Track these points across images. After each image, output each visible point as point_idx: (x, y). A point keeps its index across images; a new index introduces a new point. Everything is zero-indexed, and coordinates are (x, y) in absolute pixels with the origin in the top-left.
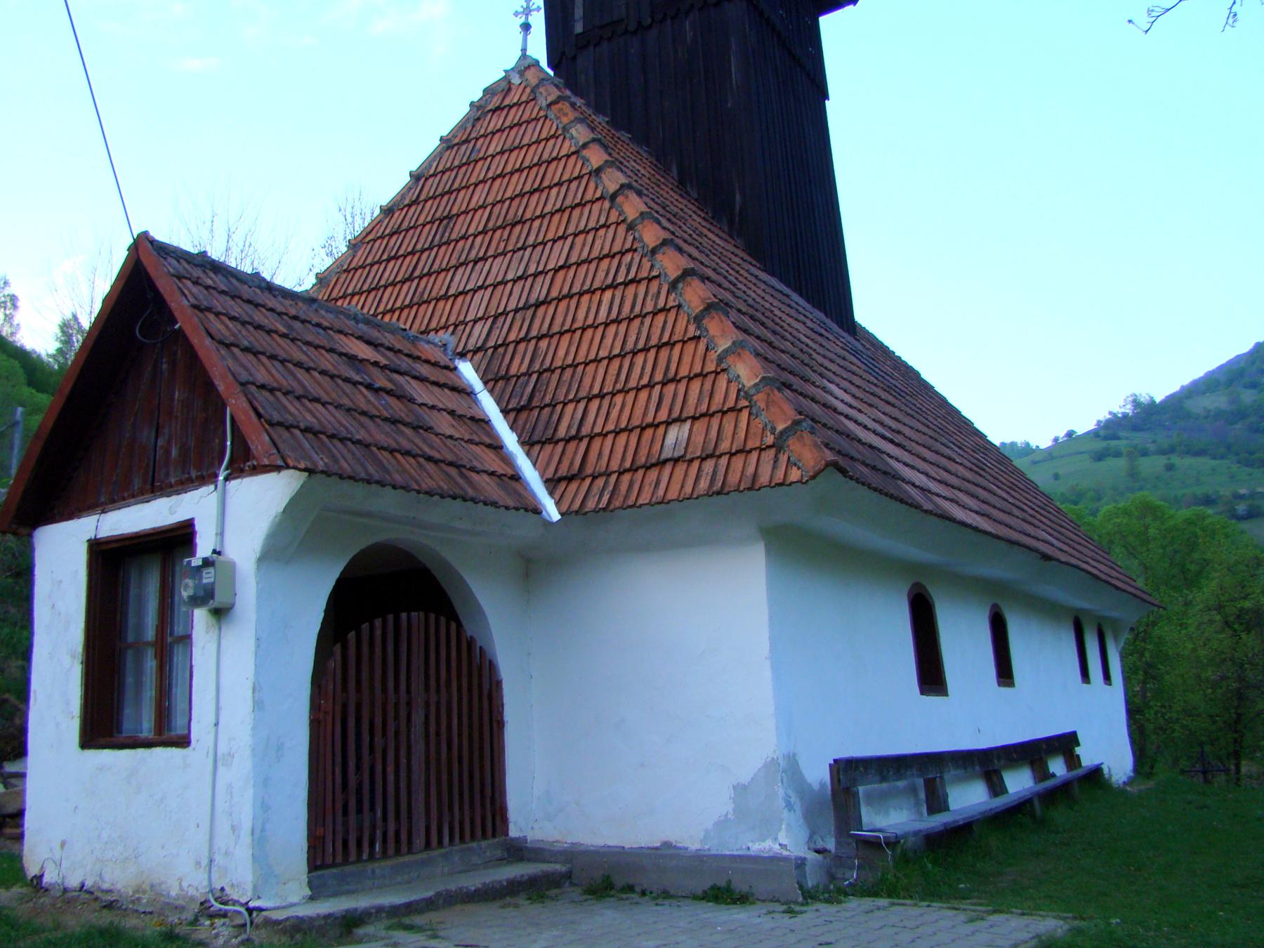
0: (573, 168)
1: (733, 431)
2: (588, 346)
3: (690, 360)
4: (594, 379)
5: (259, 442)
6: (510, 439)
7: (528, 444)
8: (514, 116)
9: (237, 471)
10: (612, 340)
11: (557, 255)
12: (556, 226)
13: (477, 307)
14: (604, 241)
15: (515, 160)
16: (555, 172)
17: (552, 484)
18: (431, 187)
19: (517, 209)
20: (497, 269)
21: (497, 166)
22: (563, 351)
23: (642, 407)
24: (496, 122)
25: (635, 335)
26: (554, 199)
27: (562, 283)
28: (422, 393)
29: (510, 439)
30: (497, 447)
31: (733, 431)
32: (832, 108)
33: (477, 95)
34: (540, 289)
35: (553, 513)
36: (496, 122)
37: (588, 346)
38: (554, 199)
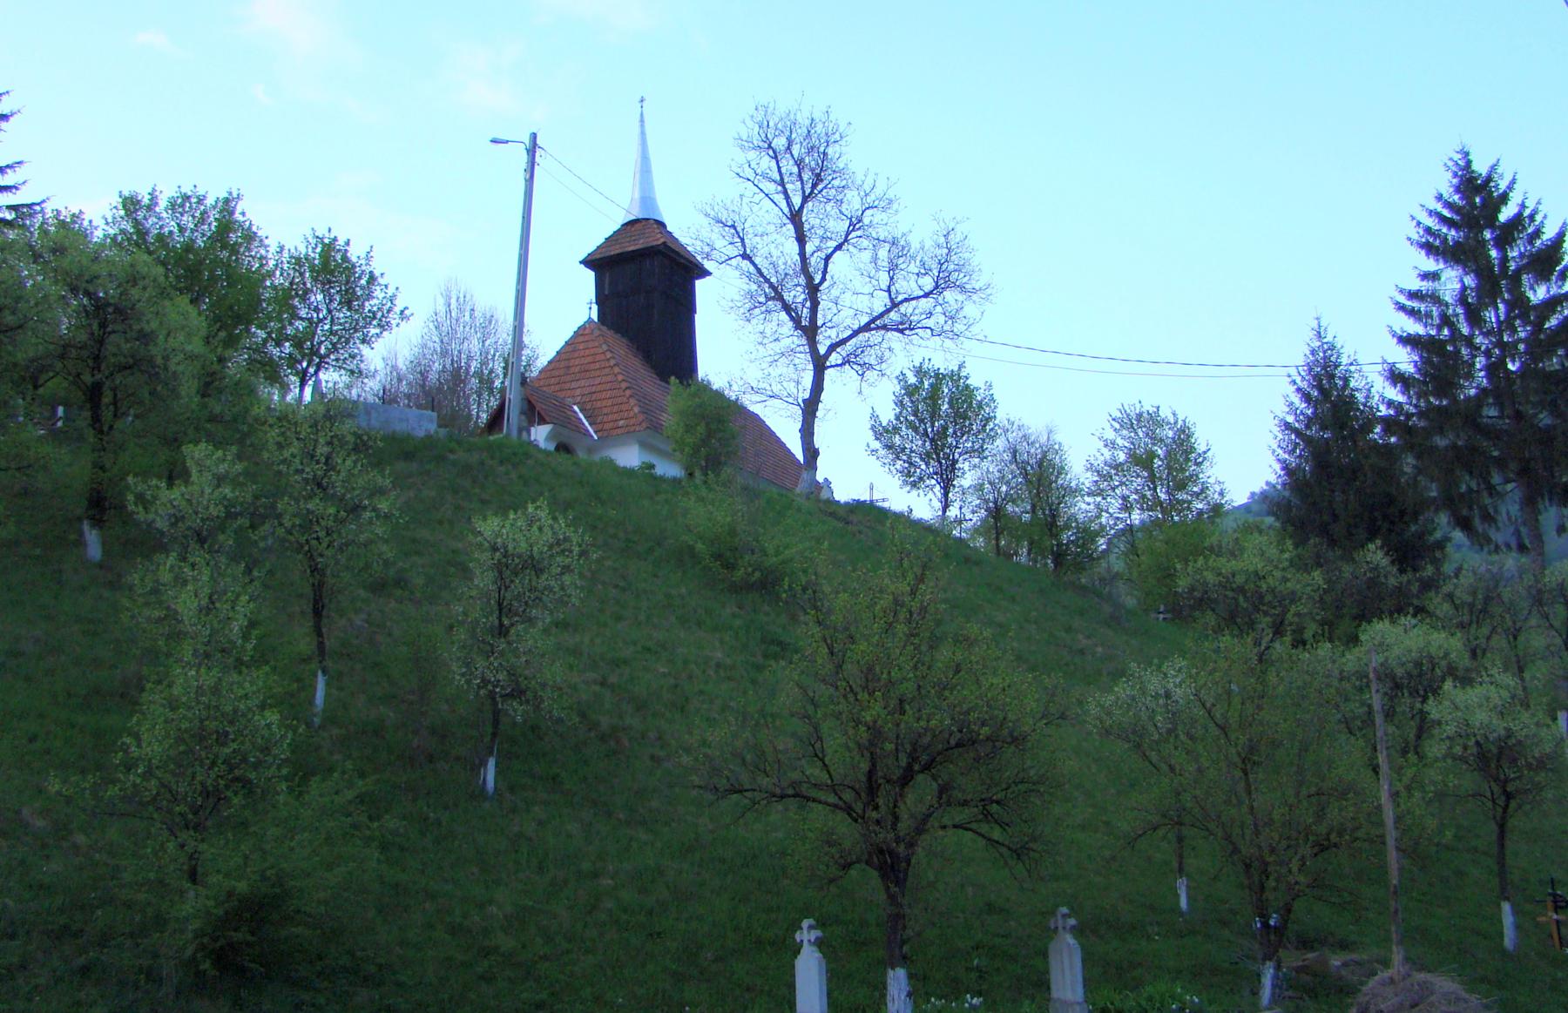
0: (603, 357)
1: (632, 421)
2: (604, 404)
3: (624, 407)
4: (605, 411)
5: (547, 419)
6: (587, 424)
7: (590, 424)
8: (586, 338)
9: (539, 424)
10: (610, 403)
11: (597, 381)
12: (598, 373)
13: (578, 392)
14: (609, 378)
15: (587, 352)
16: (598, 358)
17: (595, 432)
18: (564, 356)
19: (587, 368)
20: (582, 383)
21: (582, 353)
22: (599, 404)
23: (615, 417)
24: (581, 339)
25: (616, 401)
26: (597, 365)
27: (599, 387)
28: (569, 413)
29: (587, 424)
30: (583, 424)
31: (632, 421)
32: (698, 318)
33: (576, 329)
34: (594, 389)
35: (596, 438)
36: (581, 339)
37: (604, 404)
38: (597, 365)
